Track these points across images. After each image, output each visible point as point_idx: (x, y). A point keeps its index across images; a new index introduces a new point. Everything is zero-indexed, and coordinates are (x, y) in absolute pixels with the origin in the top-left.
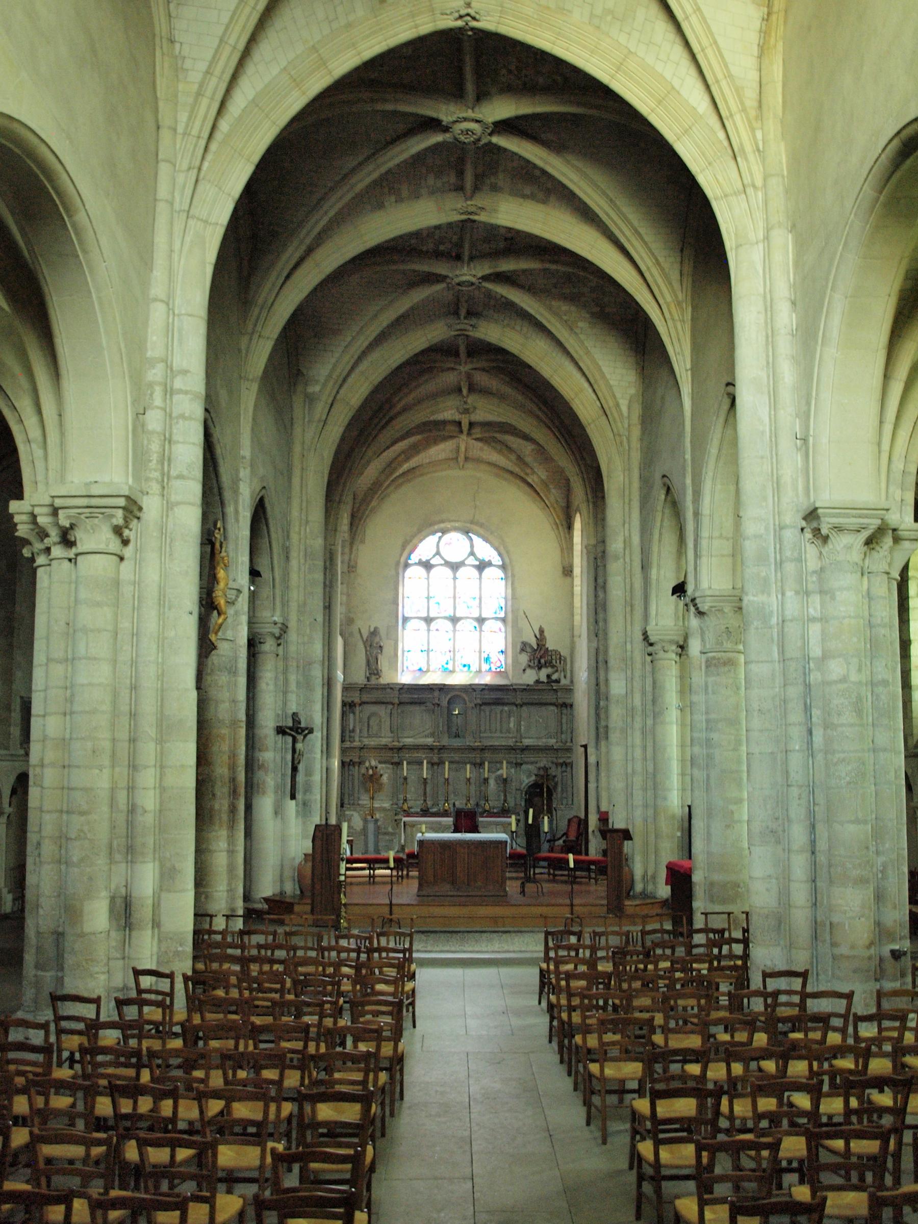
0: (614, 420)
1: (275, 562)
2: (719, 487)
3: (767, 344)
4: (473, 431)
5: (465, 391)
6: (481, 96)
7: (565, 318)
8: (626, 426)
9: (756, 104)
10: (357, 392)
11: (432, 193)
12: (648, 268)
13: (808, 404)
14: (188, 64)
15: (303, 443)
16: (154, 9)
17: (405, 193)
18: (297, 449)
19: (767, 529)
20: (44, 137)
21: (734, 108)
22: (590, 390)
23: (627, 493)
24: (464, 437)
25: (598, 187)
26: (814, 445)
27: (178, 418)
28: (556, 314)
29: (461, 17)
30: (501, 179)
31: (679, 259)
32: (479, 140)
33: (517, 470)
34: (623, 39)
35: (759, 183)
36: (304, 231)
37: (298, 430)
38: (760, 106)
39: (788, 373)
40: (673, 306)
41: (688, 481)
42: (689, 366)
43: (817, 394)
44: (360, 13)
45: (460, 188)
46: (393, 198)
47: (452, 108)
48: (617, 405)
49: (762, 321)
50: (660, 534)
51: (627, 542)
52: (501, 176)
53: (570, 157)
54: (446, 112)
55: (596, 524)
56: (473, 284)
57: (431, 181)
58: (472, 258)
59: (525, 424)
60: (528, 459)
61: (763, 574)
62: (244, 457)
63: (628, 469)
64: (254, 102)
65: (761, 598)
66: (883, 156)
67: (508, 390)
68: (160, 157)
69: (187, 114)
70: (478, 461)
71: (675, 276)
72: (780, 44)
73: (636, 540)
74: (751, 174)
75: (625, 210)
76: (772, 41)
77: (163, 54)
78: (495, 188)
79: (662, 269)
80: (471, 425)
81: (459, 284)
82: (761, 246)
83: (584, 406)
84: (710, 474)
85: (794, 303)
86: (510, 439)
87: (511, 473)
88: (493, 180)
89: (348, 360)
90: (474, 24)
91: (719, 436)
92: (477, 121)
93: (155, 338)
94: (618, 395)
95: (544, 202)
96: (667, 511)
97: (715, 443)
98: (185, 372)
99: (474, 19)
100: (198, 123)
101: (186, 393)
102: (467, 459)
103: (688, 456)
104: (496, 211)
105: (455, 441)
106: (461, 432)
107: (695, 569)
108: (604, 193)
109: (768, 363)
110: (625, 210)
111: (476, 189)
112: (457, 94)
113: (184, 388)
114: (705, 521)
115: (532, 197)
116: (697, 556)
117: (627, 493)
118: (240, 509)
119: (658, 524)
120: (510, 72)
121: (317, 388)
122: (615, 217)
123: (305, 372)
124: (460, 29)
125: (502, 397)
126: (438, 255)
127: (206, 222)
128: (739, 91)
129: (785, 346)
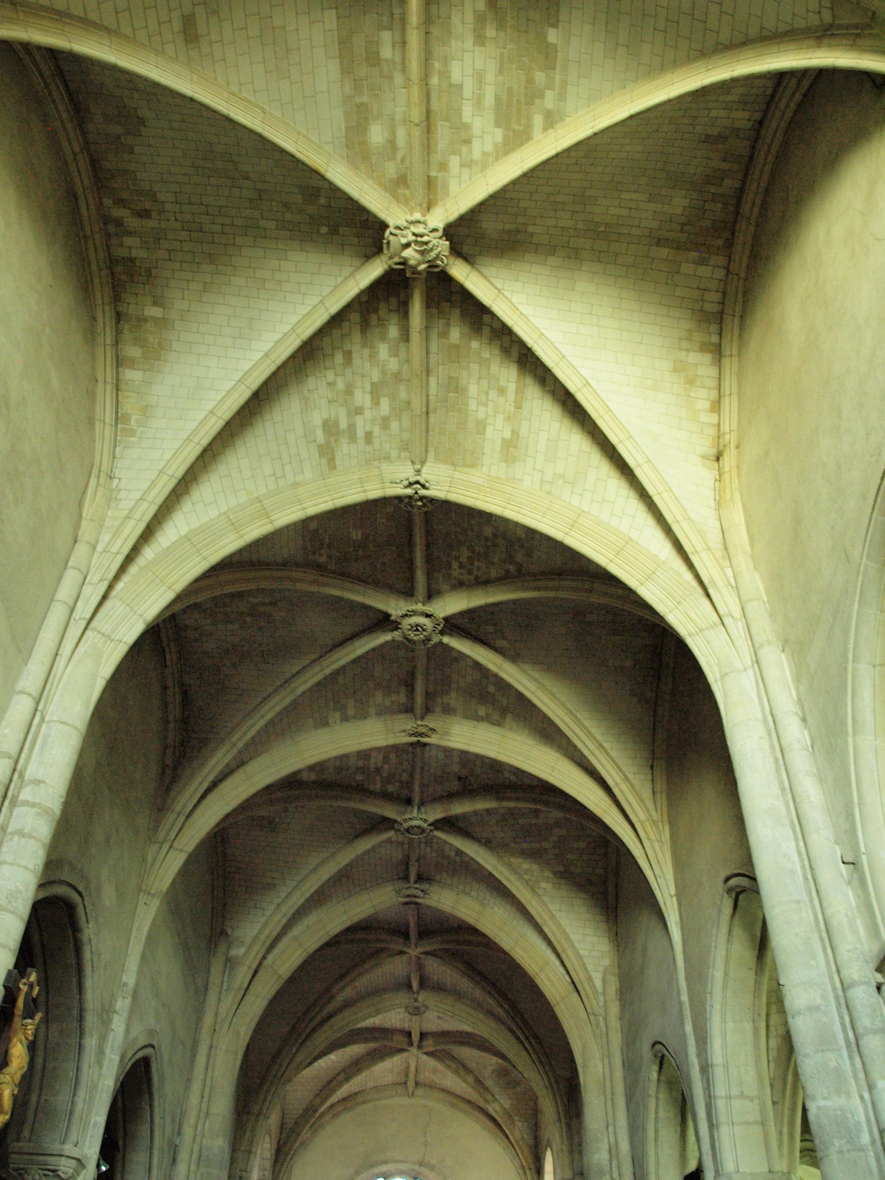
0: (587, 995)
1: (155, 1160)
2: (730, 1025)
3: (778, 770)
4: (425, 1043)
5: (415, 985)
6: (431, 595)
7: (526, 877)
8: (602, 1003)
10: (288, 959)
11: (379, 714)
12: (617, 784)
13: (850, 816)
14: (122, 495)
15: (216, 1014)
16: (98, 445)
17: (351, 712)
18: (208, 1019)
19: (824, 996)
21: (699, 547)
22: (557, 963)
23: (608, 1084)
24: (414, 1050)
25: (557, 699)
26: (869, 864)
27: (12, 834)
28: (514, 870)
30: (454, 699)
31: (649, 777)
32: (428, 639)
33: (475, 1097)
35: (737, 613)
36: (237, 736)
37: (212, 998)
38: (726, 549)
39: (812, 793)
40: (647, 824)
41: (689, 1028)
42: (673, 892)
43: (860, 798)
45: (409, 710)
46: (338, 715)
48: (590, 979)
49: (767, 747)
50: (656, 1131)
51: (613, 1151)
52: (453, 695)
53: (526, 667)
54: (395, 607)
55: (571, 1152)
56: (423, 831)
57: (379, 698)
58: (422, 803)
59: (485, 1028)
60: (489, 1083)
61: (832, 1064)
62: (125, 985)
63: (608, 1056)
64: (187, 538)
65: (837, 1102)
67: (465, 984)
68: (70, 564)
69: (110, 535)
70: (431, 1086)
71: (646, 793)
72: (737, 496)
73: (624, 1146)
74: (727, 606)
75: (587, 723)
76: (728, 495)
77: (98, 484)
78: (448, 710)
79: (632, 786)
80: (423, 1035)
81: (408, 830)
82: (750, 672)
83: (551, 981)
84: (717, 1006)
85: (804, 720)
86: (467, 1053)
87: (469, 1102)
88: (445, 699)
89: (279, 920)
90: (423, 492)
91: (723, 953)
92: (428, 616)
93: (6, 731)
94: (590, 968)
95: (499, 724)
96: (662, 1096)
97: (720, 962)
98: (38, 782)
99: (423, 487)
100: (119, 542)
101: (33, 805)
102: (417, 1084)
103: (685, 998)
104: (447, 733)
105: (405, 1054)
106: (411, 1044)
107: (713, 1147)
108: (563, 705)
109: (783, 789)
110: (587, 723)
111: (428, 710)
112: (408, 593)
113: (31, 800)
114: (718, 1074)
115: (487, 719)
116: (713, 1126)
117: (608, 1084)
118: (108, 1051)
119: (652, 1116)
120: (461, 566)
121: (242, 951)
122: (577, 729)
123: (229, 933)
124: (410, 497)
125: (458, 994)
126: (386, 796)
127: (109, 637)
129: (802, 763)
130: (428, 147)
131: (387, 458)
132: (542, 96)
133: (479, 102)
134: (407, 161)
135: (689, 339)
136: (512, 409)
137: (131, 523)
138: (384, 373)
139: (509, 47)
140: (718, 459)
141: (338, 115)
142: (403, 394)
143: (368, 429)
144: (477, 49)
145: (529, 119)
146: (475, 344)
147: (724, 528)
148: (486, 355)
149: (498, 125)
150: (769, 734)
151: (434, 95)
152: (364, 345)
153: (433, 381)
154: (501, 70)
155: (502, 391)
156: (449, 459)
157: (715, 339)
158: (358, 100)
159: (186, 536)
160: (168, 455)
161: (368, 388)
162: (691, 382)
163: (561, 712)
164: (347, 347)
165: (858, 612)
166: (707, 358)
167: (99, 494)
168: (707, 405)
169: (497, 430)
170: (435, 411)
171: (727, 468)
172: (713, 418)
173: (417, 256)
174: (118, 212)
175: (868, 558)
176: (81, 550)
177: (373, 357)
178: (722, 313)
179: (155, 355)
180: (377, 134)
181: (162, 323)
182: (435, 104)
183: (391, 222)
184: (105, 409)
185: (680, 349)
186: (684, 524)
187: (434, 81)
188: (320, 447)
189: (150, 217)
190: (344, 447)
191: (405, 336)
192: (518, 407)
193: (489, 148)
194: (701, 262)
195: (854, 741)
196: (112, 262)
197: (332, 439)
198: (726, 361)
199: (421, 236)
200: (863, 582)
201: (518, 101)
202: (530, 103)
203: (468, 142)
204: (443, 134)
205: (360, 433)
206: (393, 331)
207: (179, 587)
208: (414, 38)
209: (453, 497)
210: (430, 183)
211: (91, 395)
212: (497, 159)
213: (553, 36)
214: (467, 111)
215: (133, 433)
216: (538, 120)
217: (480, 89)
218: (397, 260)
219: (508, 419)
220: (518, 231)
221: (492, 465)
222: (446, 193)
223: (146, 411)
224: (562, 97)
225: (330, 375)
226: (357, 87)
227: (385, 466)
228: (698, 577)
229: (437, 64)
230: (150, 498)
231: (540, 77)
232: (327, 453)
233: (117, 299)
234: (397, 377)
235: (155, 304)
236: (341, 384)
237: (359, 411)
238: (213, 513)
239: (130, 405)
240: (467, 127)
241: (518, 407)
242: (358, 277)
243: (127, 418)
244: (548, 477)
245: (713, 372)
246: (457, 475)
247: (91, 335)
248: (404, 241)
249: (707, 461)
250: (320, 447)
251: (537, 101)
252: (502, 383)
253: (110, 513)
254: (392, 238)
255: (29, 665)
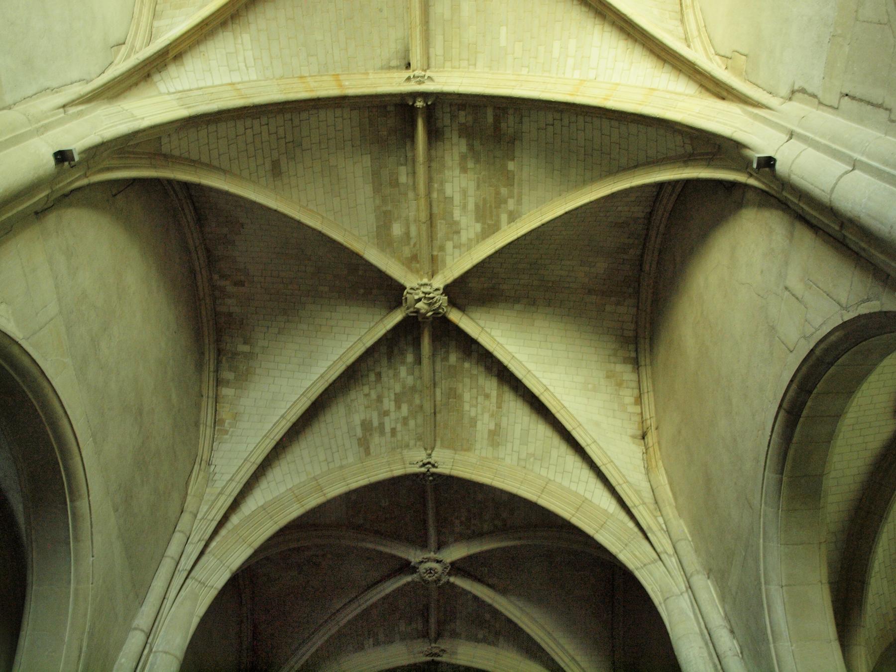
6: (440, 547)
9: (652, 501)
11: (403, 639)
16: (201, 441)
17: (381, 637)
20: (69, 412)
25: (537, 622)
29: (424, 465)
32: (439, 580)
34: (544, 473)
35: (671, 551)
36: (295, 659)
38: (656, 503)
44: (351, 460)
45: (425, 635)
47: (419, 552)
49: (706, 654)
52: (458, 622)
53: (513, 598)
54: (414, 556)
57: (403, 627)
64: (263, 508)
66: (774, 436)
72: (660, 463)
76: (654, 463)
78: (454, 635)
82: (686, 596)
90: (433, 470)
92: (438, 562)
95: (493, 644)
99: (434, 466)
110: (562, 641)
111: (439, 635)
115: (484, 640)
122: (554, 647)
124: (424, 474)
128: (638, 492)
130: (431, 237)
131: (407, 446)
132: (506, 202)
133: (464, 207)
134: (418, 246)
135: (615, 355)
136: (495, 408)
137: (223, 498)
138: (404, 387)
139: (483, 173)
140: (643, 438)
141: (372, 218)
142: (417, 401)
143: (393, 426)
144: (462, 175)
145: (498, 216)
146: (467, 365)
147: (654, 487)
148: (475, 372)
149: (477, 221)
150: (707, 644)
151: (435, 205)
152: (390, 367)
153: (438, 392)
154: (478, 187)
155: (487, 396)
156: (452, 446)
157: (633, 355)
158: (384, 209)
159: (262, 506)
160: (251, 447)
161: (393, 397)
162: (619, 385)
163: (542, 634)
164: (378, 370)
165: (764, 547)
166: (629, 367)
167: (200, 477)
168: (632, 400)
169: (485, 424)
170: (440, 412)
171: (650, 444)
172: (637, 409)
173: (426, 307)
174: (222, 283)
175: (765, 503)
176: (186, 518)
177: (396, 375)
178: (636, 337)
179: (243, 378)
180: (397, 230)
181: (250, 356)
182: (435, 210)
183: (408, 285)
184: (207, 416)
185: (610, 362)
186: (624, 486)
187: (435, 195)
188: (359, 439)
189: (244, 285)
190: (376, 439)
191: (418, 361)
192: (499, 407)
193: (472, 235)
194: (618, 304)
195: (775, 646)
196: (217, 314)
197: (368, 434)
198: (643, 370)
199: (429, 293)
200: (764, 523)
201: (491, 206)
202: (498, 207)
203: (458, 232)
204: (441, 228)
205: (388, 429)
206: (410, 358)
207: (257, 544)
208: (421, 170)
209: (455, 473)
210: (433, 259)
211: (198, 406)
212: (478, 242)
213: (511, 166)
214: (457, 214)
215: (226, 432)
216: (504, 217)
217: (465, 199)
218: (412, 310)
219: (492, 415)
220: (493, 288)
221: (482, 449)
222: (444, 264)
223: (236, 416)
224: (519, 202)
225: (366, 389)
226: (384, 201)
227: (405, 452)
228: (638, 524)
229: (436, 185)
230: (238, 478)
231: (504, 191)
232: (364, 444)
233: (218, 341)
234: (413, 389)
235: (245, 343)
236: (374, 395)
237: (386, 413)
238: (283, 489)
239: (225, 413)
240: (457, 223)
241: (499, 407)
242: (385, 322)
243: (222, 422)
244: (523, 456)
245: (634, 377)
246: (457, 457)
247: (199, 366)
248: (416, 297)
249: (637, 441)
250: (359, 439)
251: (503, 206)
252: (487, 391)
253: (208, 490)
254: (408, 295)
255: (143, 608)
